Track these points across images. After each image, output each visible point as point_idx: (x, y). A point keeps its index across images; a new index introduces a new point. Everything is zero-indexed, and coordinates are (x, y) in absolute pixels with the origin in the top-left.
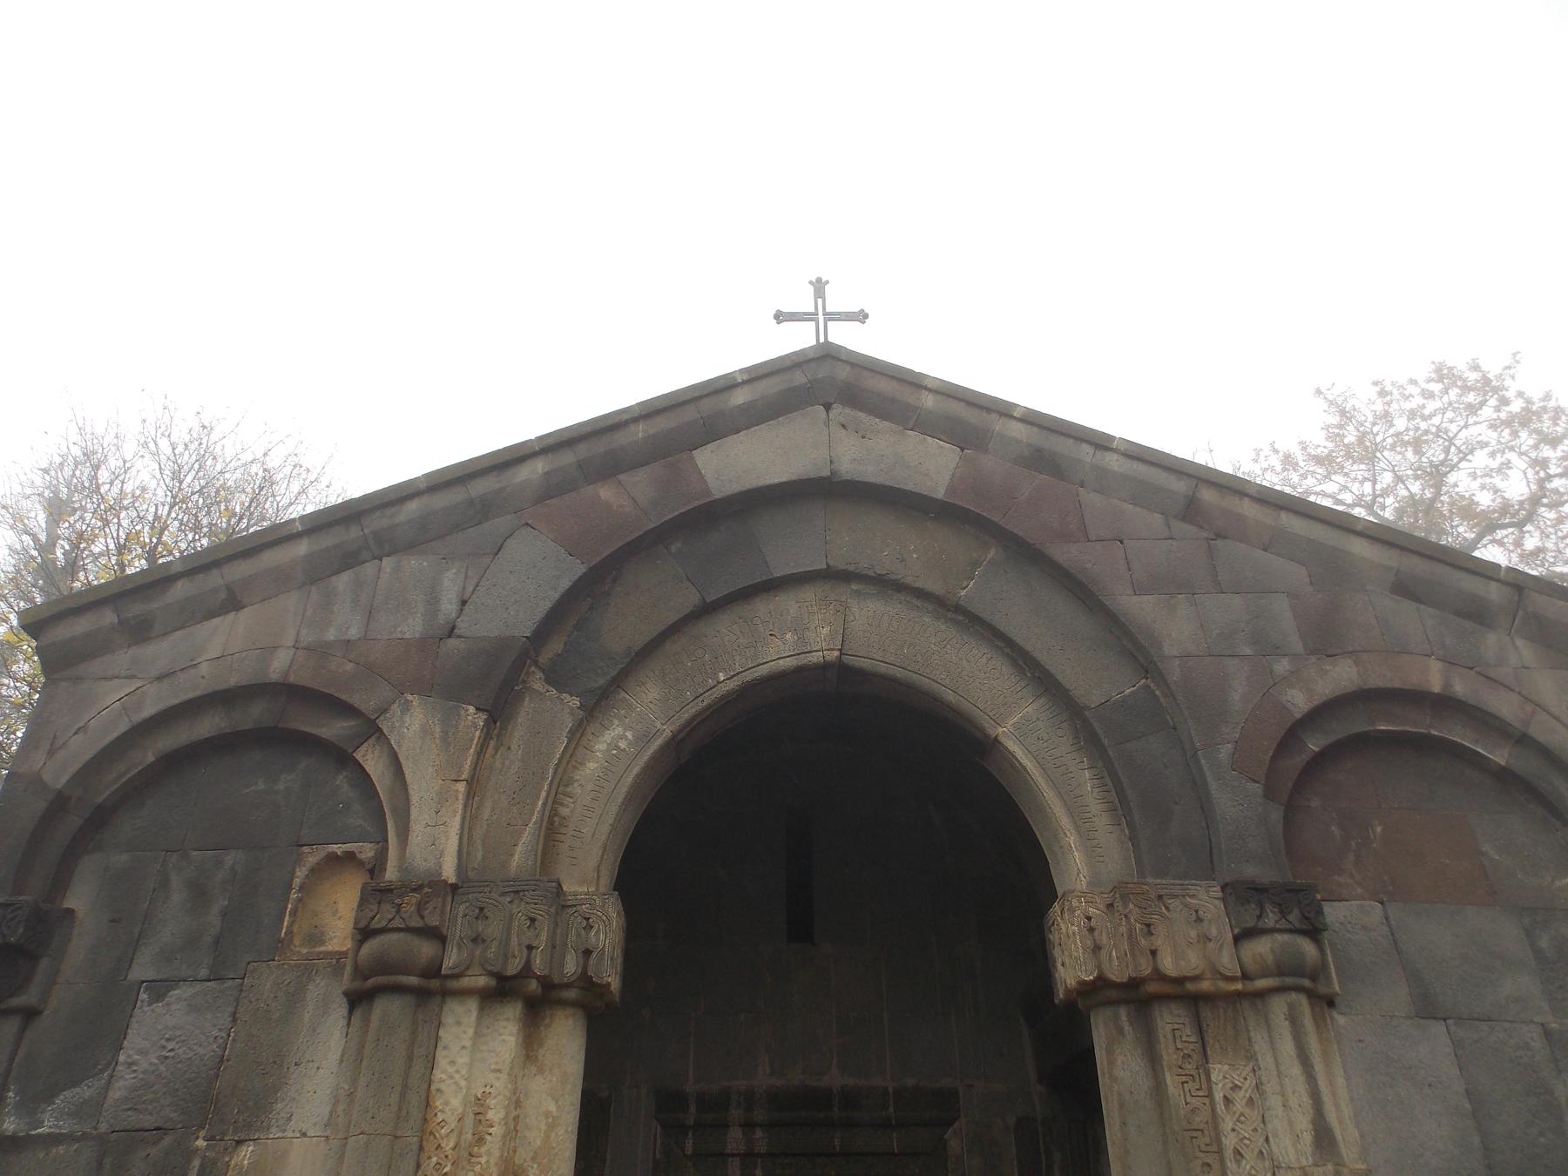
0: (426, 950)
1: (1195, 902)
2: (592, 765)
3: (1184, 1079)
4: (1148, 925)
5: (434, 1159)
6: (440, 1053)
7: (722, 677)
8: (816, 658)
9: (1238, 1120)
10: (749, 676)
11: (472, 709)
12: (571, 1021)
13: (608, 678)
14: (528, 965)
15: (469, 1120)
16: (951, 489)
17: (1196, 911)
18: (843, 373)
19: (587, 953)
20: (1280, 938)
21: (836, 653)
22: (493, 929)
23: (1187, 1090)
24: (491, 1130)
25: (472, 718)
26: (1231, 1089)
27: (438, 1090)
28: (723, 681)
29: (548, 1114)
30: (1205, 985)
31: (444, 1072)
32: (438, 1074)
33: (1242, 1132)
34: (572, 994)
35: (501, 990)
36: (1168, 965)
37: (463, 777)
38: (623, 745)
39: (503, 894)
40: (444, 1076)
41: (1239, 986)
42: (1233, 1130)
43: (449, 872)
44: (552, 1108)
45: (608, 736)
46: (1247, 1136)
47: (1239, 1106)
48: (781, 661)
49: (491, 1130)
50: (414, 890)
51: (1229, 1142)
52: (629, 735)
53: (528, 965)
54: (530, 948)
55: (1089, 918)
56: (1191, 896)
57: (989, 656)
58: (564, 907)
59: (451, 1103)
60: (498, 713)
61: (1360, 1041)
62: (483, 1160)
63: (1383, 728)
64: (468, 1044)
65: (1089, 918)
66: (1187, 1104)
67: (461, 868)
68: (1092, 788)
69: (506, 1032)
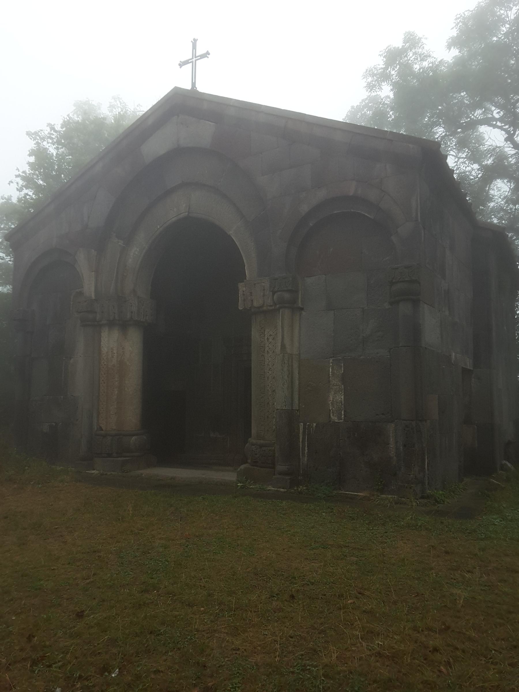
1: (264, 284)
2: (130, 260)
5: (103, 361)
6: (102, 338)
8: (181, 216)
9: (270, 344)
11: (93, 250)
17: (264, 287)
19: (132, 312)
20: (279, 293)
21: (187, 213)
23: (261, 337)
24: (115, 355)
26: (269, 336)
27: (102, 347)
28: (159, 228)
30: (265, 308)
31: (103, 342)
32: (102, 343)
33: (270, 347)
35: (111, 324)
36: (256, 304)
38: (137, 253)
40: (103, 344)
41: (273, 308)
42: (268, 346)
43: (93, 297)
46: (271, 347)
47: (270, 340)
48: (173, 219)
49: (115, 355)
51: (267, 349)
55: (244, 291)
56: (263, 283)
59: (104, 350)
61: (308, 319)
62: (114, 361)
63: (336, 212)
65: (244, 291)
66: (260, 340)
68: (253, 248)
69: (116, 334)
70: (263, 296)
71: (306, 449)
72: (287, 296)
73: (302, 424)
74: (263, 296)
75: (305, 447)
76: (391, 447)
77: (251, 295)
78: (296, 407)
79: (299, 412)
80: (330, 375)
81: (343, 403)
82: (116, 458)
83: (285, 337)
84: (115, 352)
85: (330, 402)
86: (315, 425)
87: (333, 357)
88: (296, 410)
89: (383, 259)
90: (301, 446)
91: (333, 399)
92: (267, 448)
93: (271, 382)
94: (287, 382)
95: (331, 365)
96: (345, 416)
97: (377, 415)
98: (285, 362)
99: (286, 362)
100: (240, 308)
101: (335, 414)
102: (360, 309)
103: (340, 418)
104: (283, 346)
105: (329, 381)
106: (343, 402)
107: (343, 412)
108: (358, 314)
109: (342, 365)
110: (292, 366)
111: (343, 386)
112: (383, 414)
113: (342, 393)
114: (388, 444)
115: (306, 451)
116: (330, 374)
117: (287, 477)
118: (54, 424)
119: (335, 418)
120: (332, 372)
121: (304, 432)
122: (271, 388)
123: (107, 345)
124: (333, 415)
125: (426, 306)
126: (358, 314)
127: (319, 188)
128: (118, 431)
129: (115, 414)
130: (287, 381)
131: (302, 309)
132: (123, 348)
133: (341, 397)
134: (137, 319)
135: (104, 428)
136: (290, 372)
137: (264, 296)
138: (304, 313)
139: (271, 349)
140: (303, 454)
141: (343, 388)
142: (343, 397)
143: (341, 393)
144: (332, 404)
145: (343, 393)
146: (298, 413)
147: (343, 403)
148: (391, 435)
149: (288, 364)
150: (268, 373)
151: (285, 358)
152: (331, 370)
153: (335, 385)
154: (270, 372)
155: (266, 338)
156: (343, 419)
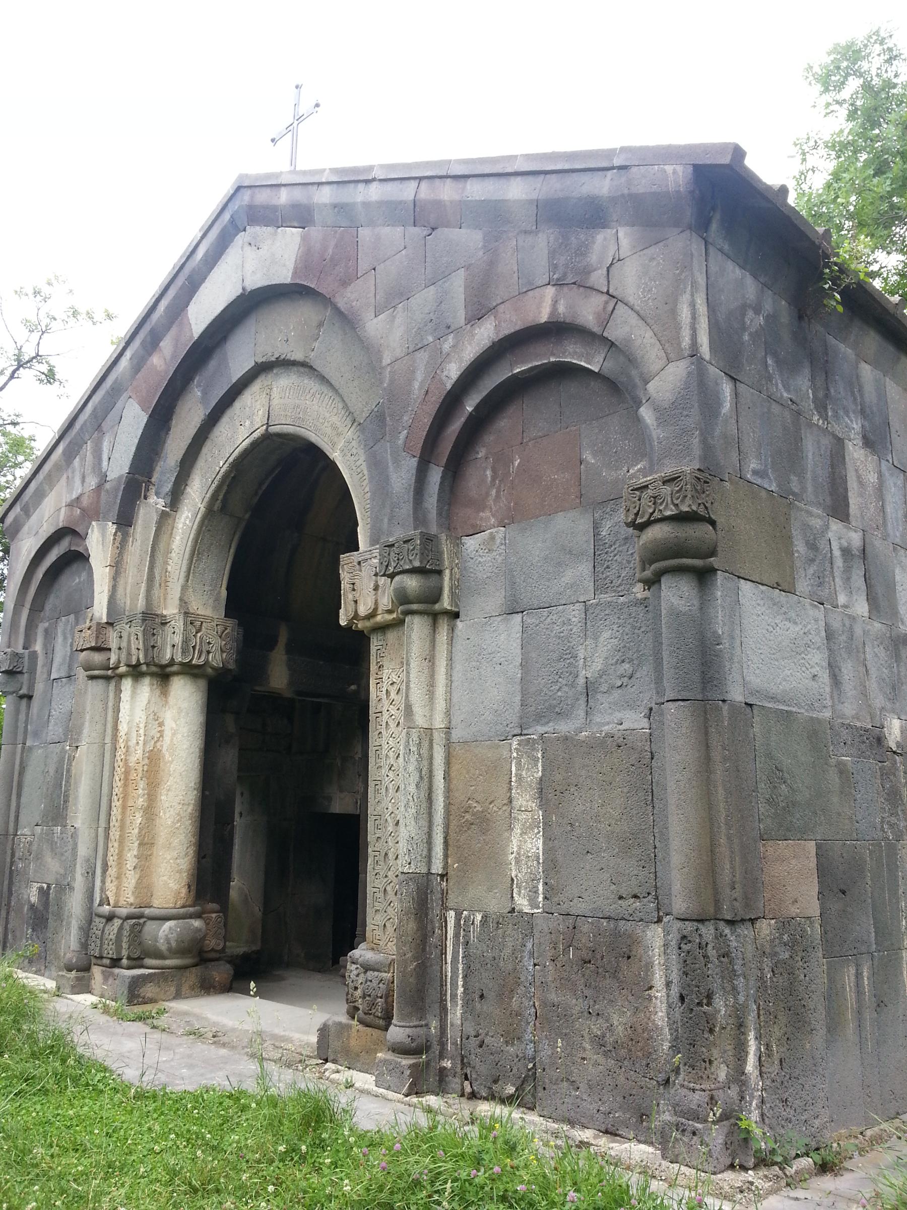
0: (97, 657)
3: (378, 681)
4: (353, 584)
7: (221, 464)
8: (256, 435)
10: (231, 459)
12: (182, 681)
13: (172, 483)
14: (138, 660)
15: (134, 734)
16: (295, 273)
18: (245, 197)
19: (174, 646)
21: (265, 427)
22: (124, 645)
25: (111, 528)
29: (172, 729)
30: (379, 618)
32: (121, 715)
34: (175, 668)
35: (136, 672)
37: (108, 564)
39: (127, 624)
44: (174, 725)
45: (182, 520)
46: (393, 713)
47: (393, 695)
50: (89, 629)
52: (190, 515)
53: (138, 660)
54: (138, 649)
57: (332, 398)
58: (164, 624)
60: (125, 521)
61: (468, 639)
64: (129, 699)
66: (377, 697)
67: (109, 614)
70: (374, 590)
71: (460, 983)
72: (412, 583)
73: (452, 914)
74: (374, 590)
75: (458, 977)
76: (656, 998)
77: (354, 590)
78: (437, 867)
79: (447, 880)
80: (513, 784)
81: (541, 861)
82: (128, 969)
83: (412, 686)
84: (142, 732)
85: (513, 855)
86: (479, 917)
87: (521, 735)
88: (438, 875)
89: (628, 472)
90: (449, 974)
91: (520, 848)
92: (376, 973)
93: (393, 801)
94: (416, 800)
95: (515, 755)
96: (545, 898)
97: (621, 898)
98: (411, 748)
99: (413, 749)
100: (343, 622)
101: (523, 891)
102: (578, 604)
103: (533, 904)
104: (409, 710)
105: (510, 801)
106: (541, 857)
107: (541, 887)
108: (574, 619)
109: (539, 755)
110: (431, 758)
111: (541, 813)
112: (635, 896)
113: (539, 832)
114: (651, 988)
115: (461, 990)
116: (513, 779)
117: (406, 1061)
118: (45, 886)
119: (522, 903)
120: (516, 775)
121: (456, 935)
122: (392, 815)
123: (127, 718)
124: (519, 893)
125: (746, 587)
126: (574, 619)
127: (479, 319)
128: (140, 907)
129: (135, 868)
130: (415, 798)
131: (456, 615)
132: (161, 724)
133: (536, 844)
134: (180, 660)
135: (112, 902)
136: (423, 773)
137: (376, 588)
138: (459, 624)
139: (393, 717)
140: (454, 996)
141: (541, 817)
142: (541, 842)
143: (536, 831)
144: (518, 861)
145: (541, 833)
146: (445, 884)
147: (541, 861)
148: (657, 962)
149: (420, 755)
150: (387, 776)
151: (411, 739)
152: (514, 769)
153: (523, 809)
154: (391, 774)
155: (384, 690)
156: (541, 905)
